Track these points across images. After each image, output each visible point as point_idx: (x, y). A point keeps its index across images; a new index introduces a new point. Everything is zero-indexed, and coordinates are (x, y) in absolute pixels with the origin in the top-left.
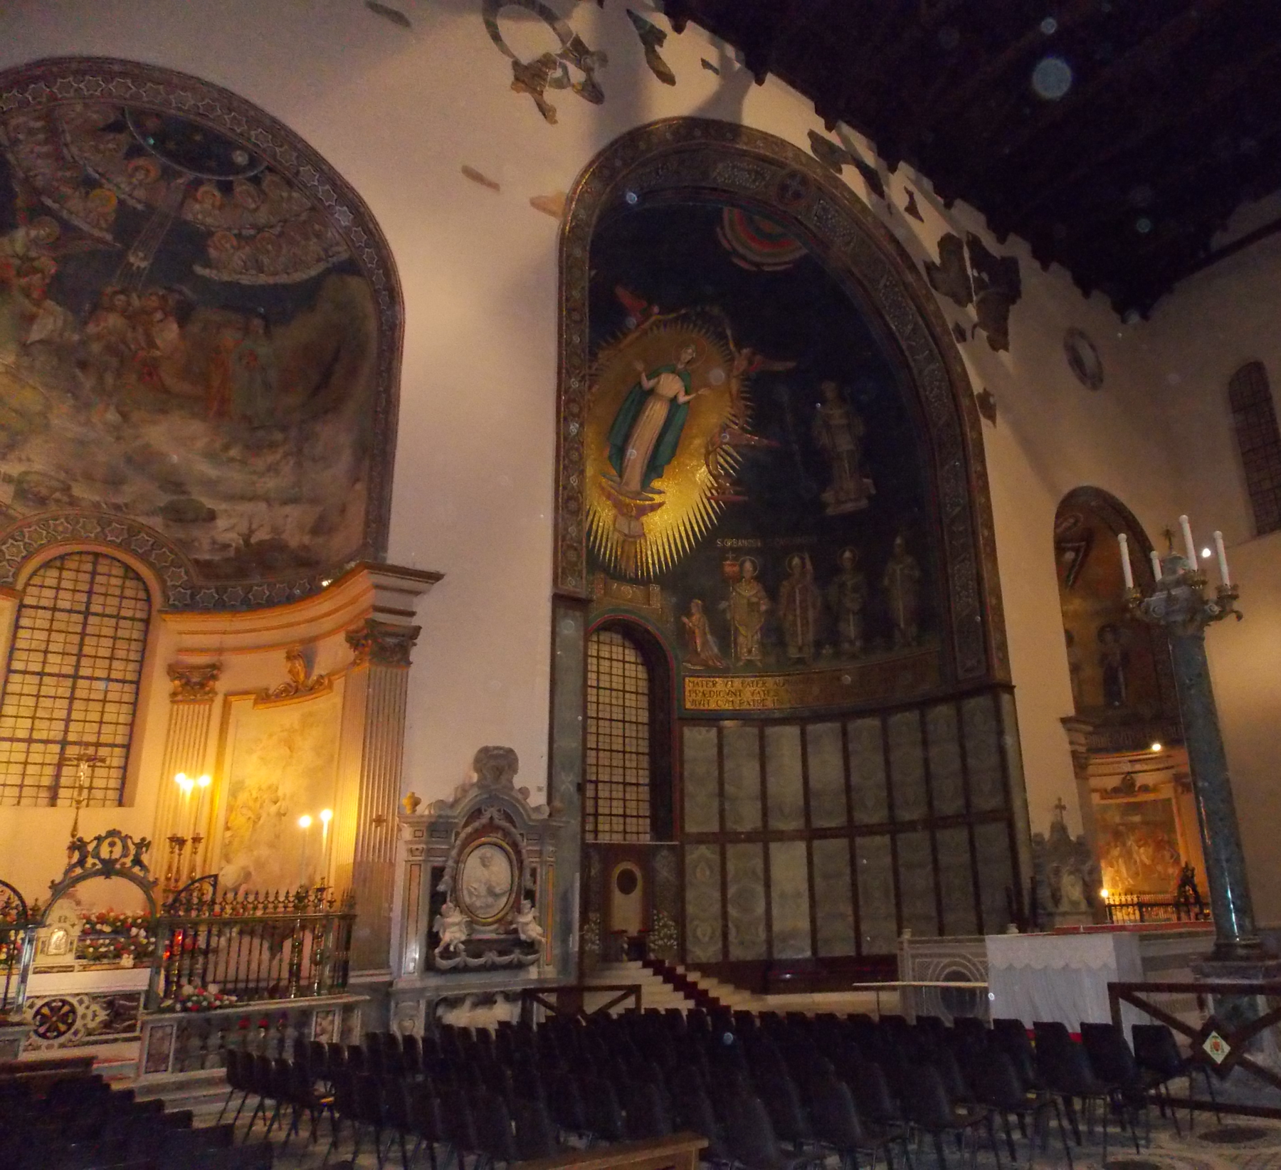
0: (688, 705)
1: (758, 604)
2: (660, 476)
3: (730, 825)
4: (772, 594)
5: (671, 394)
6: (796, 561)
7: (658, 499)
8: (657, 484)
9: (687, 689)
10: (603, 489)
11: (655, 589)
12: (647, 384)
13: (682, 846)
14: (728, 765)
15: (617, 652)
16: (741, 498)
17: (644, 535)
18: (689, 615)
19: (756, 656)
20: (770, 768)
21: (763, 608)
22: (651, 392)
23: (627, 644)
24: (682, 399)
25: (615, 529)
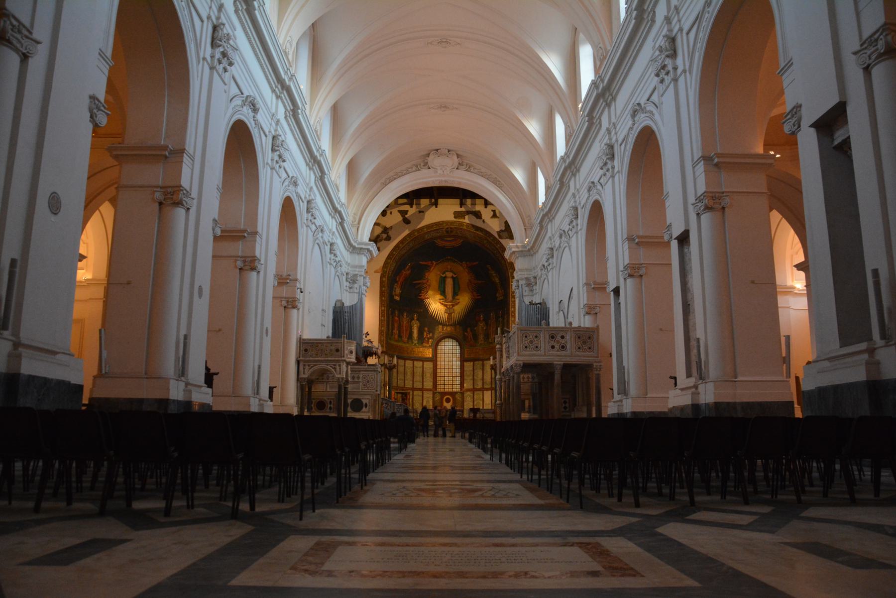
0: (466, 357)
1: (483, 327)
2: (458, 295)
3: (475, 387)
4: (487, 324)
5: (451, 276)
6: (492, 314)
7: (458, 301)
8: (457, 297)
9: (466, 352)
10: (440, 303)
11: (458, 326)
12: (444, 275)
13: (463, 392)
14: (475, 371)
15: (451, 344)
16: (479, 297)
17: (454, 312)
18: (467, 332)
19: (483, 342)
20: (485, 372)
21: (485, 328)
22: (446, 277)
23: (454, 341)
24: (455, 276)
25: (445, 312)
